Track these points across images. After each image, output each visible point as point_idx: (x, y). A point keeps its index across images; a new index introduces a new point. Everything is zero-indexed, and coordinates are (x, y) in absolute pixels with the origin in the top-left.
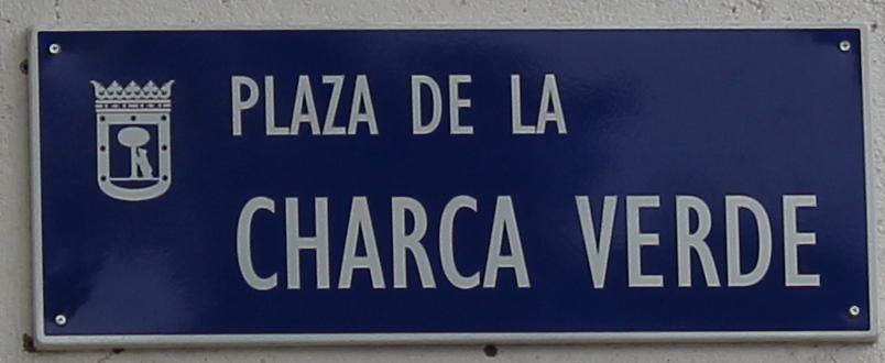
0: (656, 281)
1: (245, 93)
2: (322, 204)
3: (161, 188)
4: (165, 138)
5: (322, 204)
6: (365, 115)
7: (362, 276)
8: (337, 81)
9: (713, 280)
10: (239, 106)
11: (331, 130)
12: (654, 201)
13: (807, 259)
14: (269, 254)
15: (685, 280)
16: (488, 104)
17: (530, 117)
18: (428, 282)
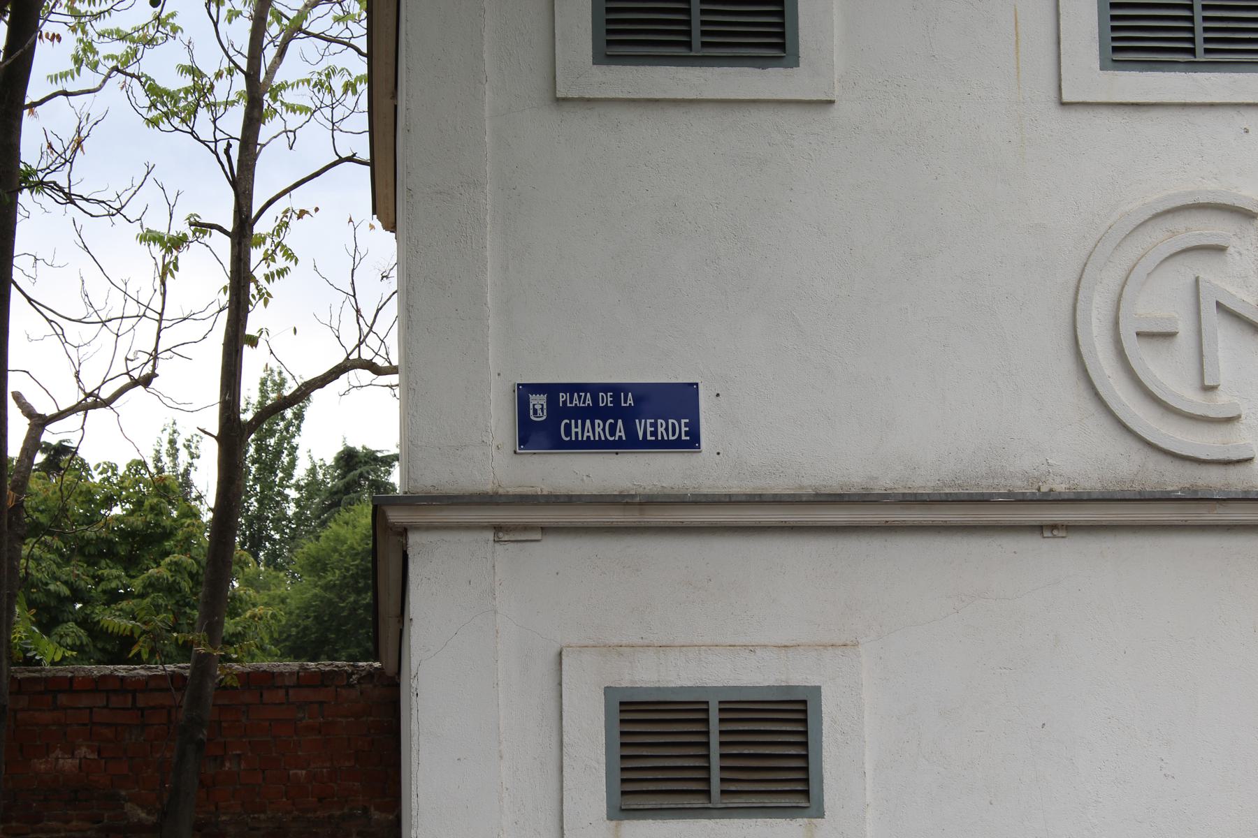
0: (653, 438)
1: (563, 397)
2: (580, 421)
3: (544, 418)
4: (545, 407)
5: (580, 421)
6: (589, 402)
7: (588, 437)
8: (583, 394)
9: (666, 438)
10: (561, 400)
11: (581, 405)
12: (653, 421)
13: (687, 434)
14: (568, 433)
15: (660, 438)
16: (616, 399)
17: (625, 402)
18: (603, 438)
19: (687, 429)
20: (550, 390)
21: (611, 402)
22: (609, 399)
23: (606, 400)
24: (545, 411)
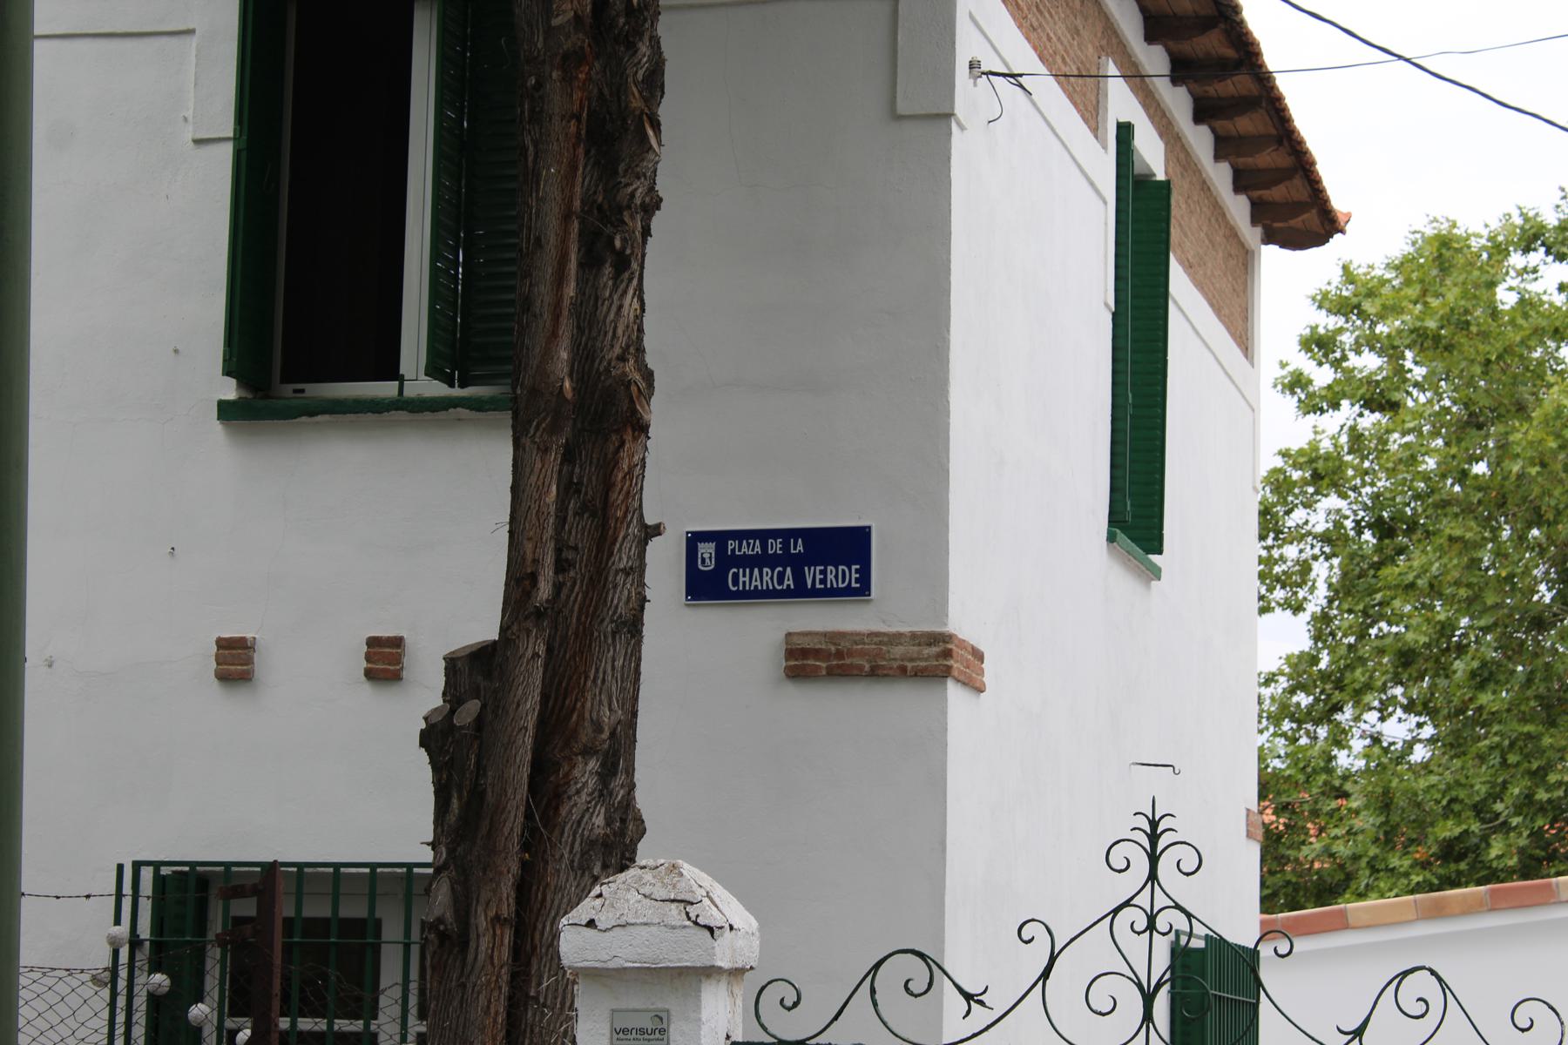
0: (822, 586)
1: (732, 544)
2: (748, 570)
3: (712, 567)
4: (713, 555)
5: (748, 570)
6: (758, 549)
7: (756, 587)
8: (752, 541)
9: (835, 586)
10: (730, 548)
11: (750, 553)
12: (822, 568)
13: (857, 581)
14: (736, 583)
15: (829, 586)
16: (786, 546)
17: (795, 549)
18: (771, 587)
19: (858, 576)
20: (719, 538)
21: (780, 549)
22: (779, 546)
23: (775, 547)
24: (713, 560)
